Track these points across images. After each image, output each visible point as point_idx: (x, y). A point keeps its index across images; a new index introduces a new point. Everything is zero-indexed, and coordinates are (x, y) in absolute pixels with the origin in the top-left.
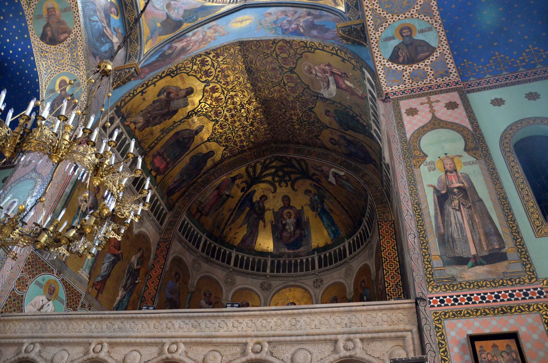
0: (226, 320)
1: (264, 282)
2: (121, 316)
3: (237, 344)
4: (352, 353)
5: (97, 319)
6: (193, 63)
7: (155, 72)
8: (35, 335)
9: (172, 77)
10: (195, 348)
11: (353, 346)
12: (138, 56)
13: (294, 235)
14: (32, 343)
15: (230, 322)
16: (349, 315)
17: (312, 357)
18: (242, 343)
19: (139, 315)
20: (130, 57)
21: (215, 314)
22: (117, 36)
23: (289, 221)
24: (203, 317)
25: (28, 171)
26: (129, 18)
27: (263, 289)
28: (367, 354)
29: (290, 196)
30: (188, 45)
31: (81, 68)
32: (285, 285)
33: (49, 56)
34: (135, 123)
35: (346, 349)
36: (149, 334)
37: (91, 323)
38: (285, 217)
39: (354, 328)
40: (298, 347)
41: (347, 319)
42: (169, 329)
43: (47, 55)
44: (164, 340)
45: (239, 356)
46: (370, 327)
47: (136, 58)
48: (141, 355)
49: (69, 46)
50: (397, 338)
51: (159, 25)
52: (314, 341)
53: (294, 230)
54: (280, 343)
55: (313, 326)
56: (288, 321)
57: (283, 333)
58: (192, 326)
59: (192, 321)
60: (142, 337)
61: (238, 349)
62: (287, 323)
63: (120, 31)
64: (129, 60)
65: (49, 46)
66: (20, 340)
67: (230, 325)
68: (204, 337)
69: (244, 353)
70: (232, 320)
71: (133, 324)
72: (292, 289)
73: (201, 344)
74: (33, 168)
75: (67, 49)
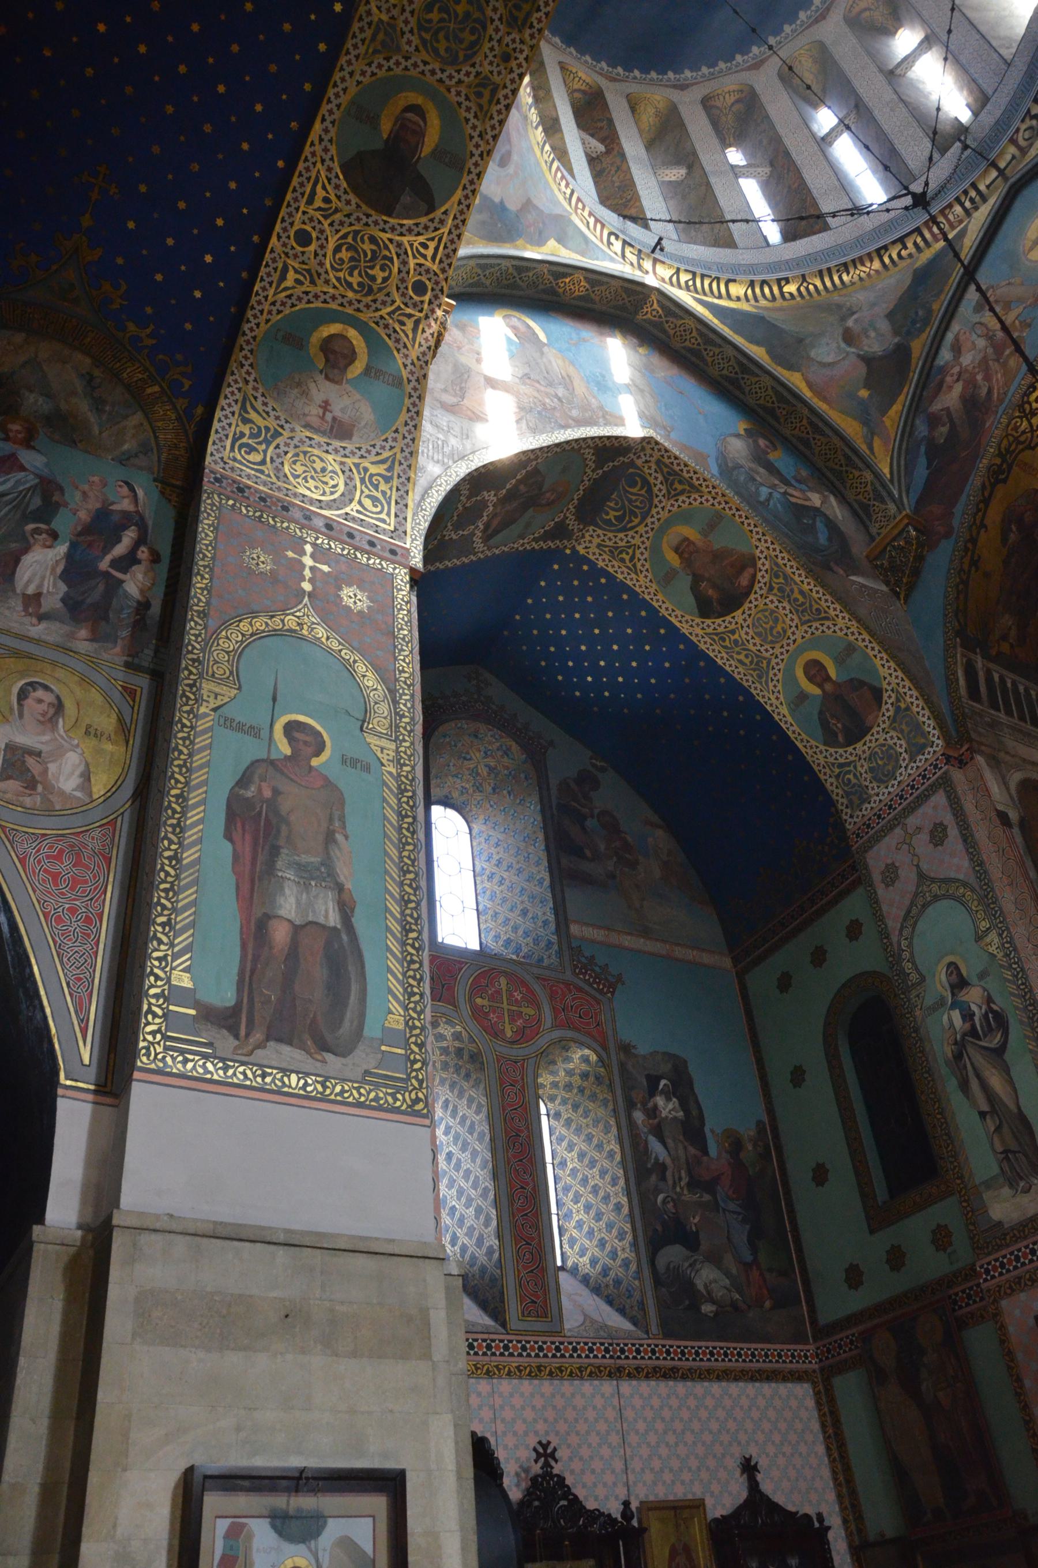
6: (1026, 416)
7: (963, 498)
9: (1005, 481)
12: (884, 494)
20: (866, 508)
22: (811, 489)
25: (911, 888)
26: (796, 432)
30: (971, 384)
31: (832, 613)
33: (744, 636)
34: (1004, 638)
43: (736, 636)
47: (883, 502)
49: (771, 588)
51: (864, 393)
63: (804, 473)
64: (869, 516)
65: (728, 618)
74: (913, 876)
75: (771, 597)
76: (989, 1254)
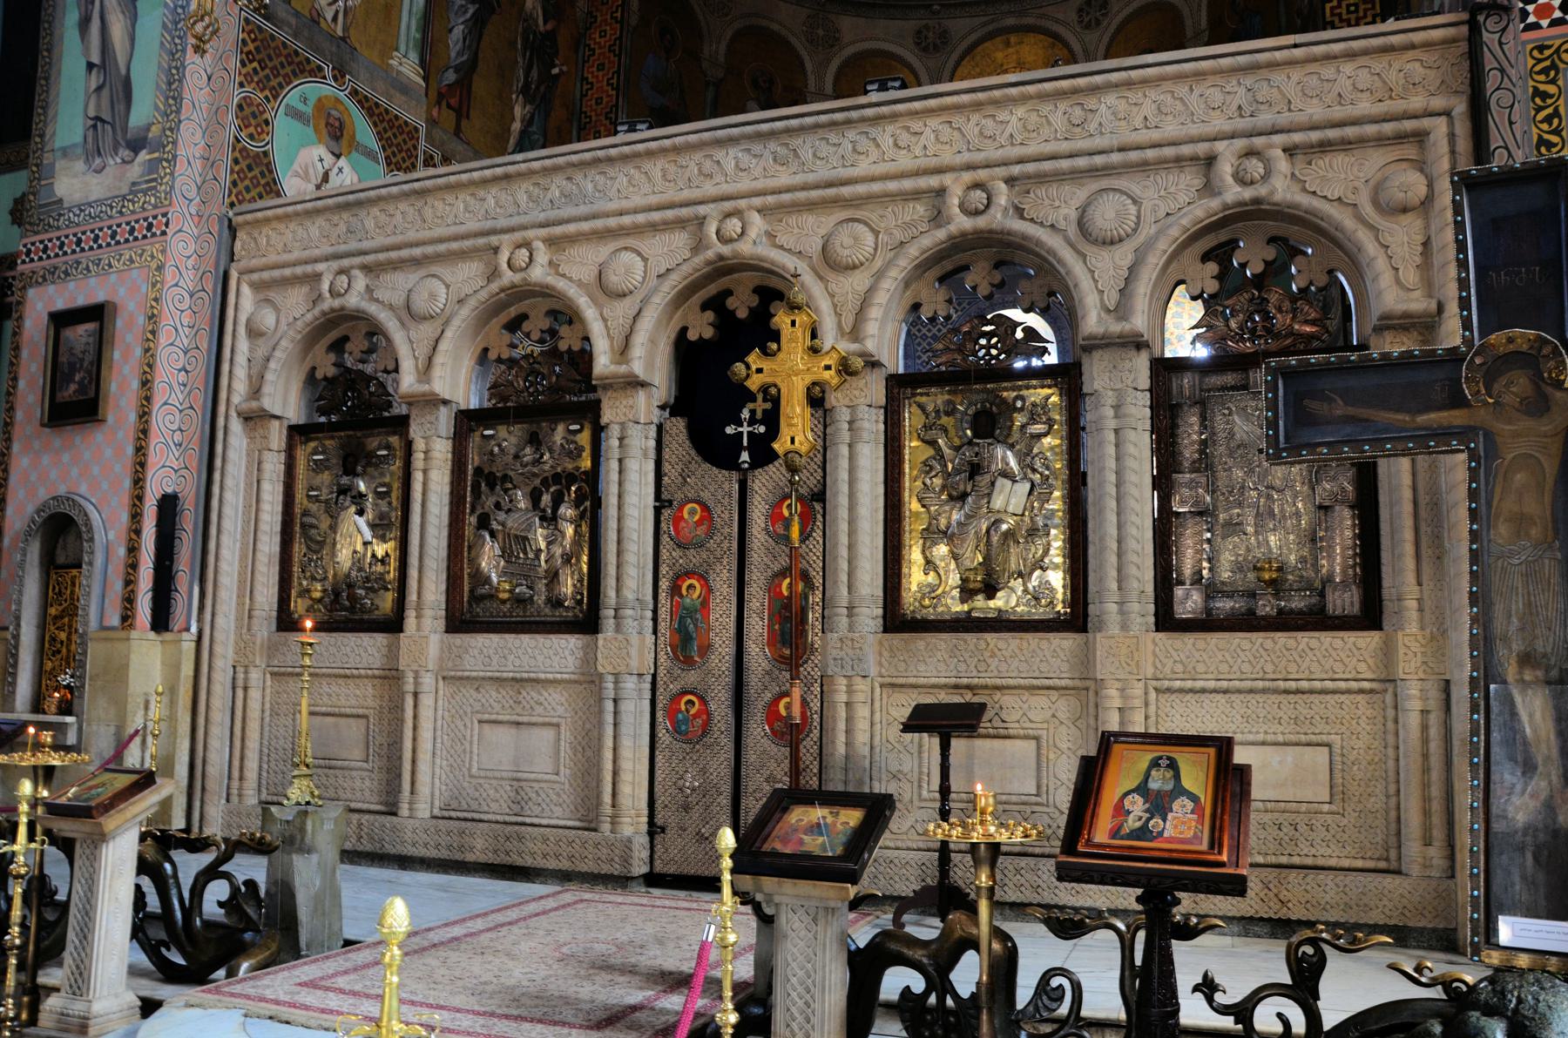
0: (874, 132)
1: (926, 27)
2: (561, 160)
3: (915, 195)
4: (1261, 191)
5: (495, 179)
8: (343, 248)
10: (792, 220)
11: (1262, 171)
14: (341, 272)
15: (886, 135)
16: (1249, 81)
17: (1139, 212)
18: (930, 191)
19: (613, 152)
21: (838, 116)
24: (802, 129)
27: (925, 50)
28: (1304, 190)
32: (990, 28)
35: (1242, 181)
36: (654, 200)
37: (481, 193)
39: (1265, 118)
40: (1095, 185)
41: (1242, 91)
42: (710, 176)
44: (702, 210)
45: (924, 227)
46: (1315, 111)
48: (645, 260)
50: (1400, 138)
52: (1143, 166)
54: (1042, 178)
55: (1138, 122)
56: (1060, 113)
57: (1049, 148)
58: (775, 160)
59: (773, 145)
60: (636, 211)
61: (920, 210)
62: (1058, 120)
66: (309, 269)
67: (887, 142)
68: (817, 187)
69: (938, 218)
70: (890, 128)
71: (600, 179)
72: (1013, 39)
73: (811, 206)
76: (36, 233)
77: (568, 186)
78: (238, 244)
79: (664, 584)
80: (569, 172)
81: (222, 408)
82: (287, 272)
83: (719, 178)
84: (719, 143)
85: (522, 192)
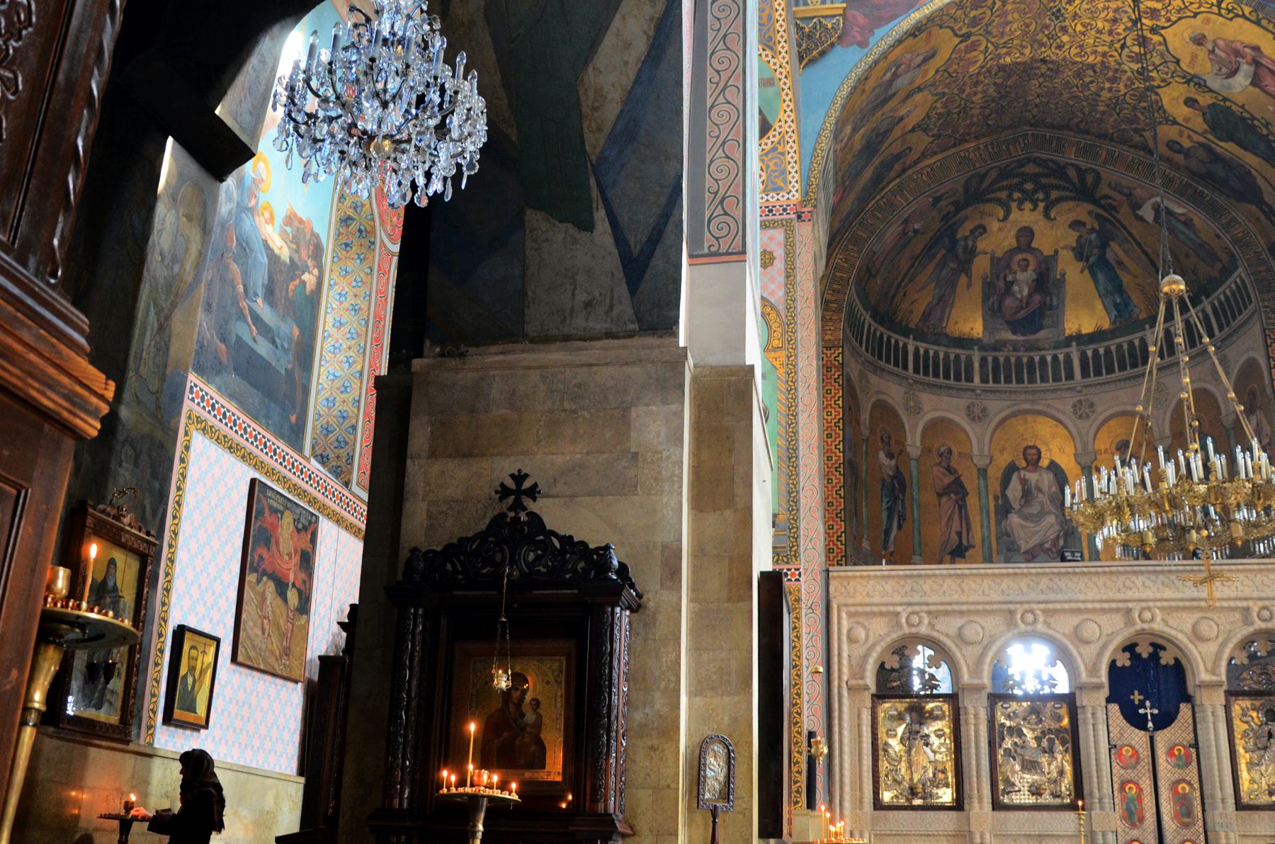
2: (1048, 570)
5: (1009, 575)
13: (1028, 303)
19: (1077, 570)
23: (1021, 276)
29: (1035, 228)
38: (1015, 267)
48: (1100, 627)
53: (1030, 296)
58: (1163, 584)
59: (1161, 577)
60: (1093, 601)
68: (1188, 600)
69: (1247, 621)
73: (1185, 609)
77: (1051, 584)
78: (832, 589)
79: (1116, 786)
80: (1051, 576)
81: (835, 683)
82: (876, 609)
83: (1136, 590)
84: (1134, 573)
85: (1023, 583)
